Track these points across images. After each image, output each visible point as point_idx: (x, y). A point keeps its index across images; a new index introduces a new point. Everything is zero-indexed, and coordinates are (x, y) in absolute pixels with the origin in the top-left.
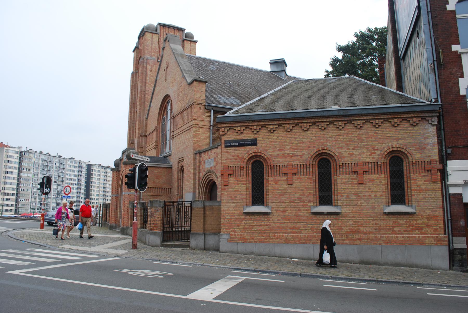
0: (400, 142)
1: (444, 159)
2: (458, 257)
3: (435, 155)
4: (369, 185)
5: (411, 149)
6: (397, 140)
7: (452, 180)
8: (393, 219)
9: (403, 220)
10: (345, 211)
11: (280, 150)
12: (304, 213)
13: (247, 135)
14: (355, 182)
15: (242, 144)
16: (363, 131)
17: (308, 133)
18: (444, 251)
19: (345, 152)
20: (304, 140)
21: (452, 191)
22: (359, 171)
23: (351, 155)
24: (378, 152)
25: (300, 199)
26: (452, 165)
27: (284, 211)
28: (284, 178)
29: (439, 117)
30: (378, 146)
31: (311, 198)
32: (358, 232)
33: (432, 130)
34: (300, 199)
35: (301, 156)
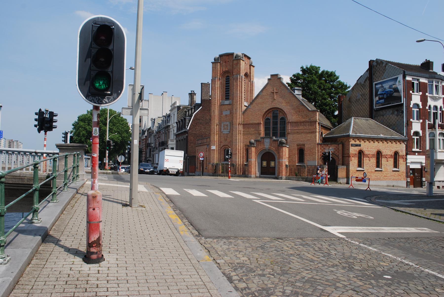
1: (407, 154)
2: (408, 184)
3: (405, 154)
5: (400, 151)
7: (408, 161)
8: (395, 172)
9: (397, 173)
12: (373, 171)
13: (358, 142)
15: (357, 145)
16: (388, 144)
18: (405, 182)
21: (408, 164)
26: (408, 156)
28: (368, 158)
29: (407, 142)
30: (392, 149)
31: (375, 165)
32: (386, 177)
33: (405, 146)
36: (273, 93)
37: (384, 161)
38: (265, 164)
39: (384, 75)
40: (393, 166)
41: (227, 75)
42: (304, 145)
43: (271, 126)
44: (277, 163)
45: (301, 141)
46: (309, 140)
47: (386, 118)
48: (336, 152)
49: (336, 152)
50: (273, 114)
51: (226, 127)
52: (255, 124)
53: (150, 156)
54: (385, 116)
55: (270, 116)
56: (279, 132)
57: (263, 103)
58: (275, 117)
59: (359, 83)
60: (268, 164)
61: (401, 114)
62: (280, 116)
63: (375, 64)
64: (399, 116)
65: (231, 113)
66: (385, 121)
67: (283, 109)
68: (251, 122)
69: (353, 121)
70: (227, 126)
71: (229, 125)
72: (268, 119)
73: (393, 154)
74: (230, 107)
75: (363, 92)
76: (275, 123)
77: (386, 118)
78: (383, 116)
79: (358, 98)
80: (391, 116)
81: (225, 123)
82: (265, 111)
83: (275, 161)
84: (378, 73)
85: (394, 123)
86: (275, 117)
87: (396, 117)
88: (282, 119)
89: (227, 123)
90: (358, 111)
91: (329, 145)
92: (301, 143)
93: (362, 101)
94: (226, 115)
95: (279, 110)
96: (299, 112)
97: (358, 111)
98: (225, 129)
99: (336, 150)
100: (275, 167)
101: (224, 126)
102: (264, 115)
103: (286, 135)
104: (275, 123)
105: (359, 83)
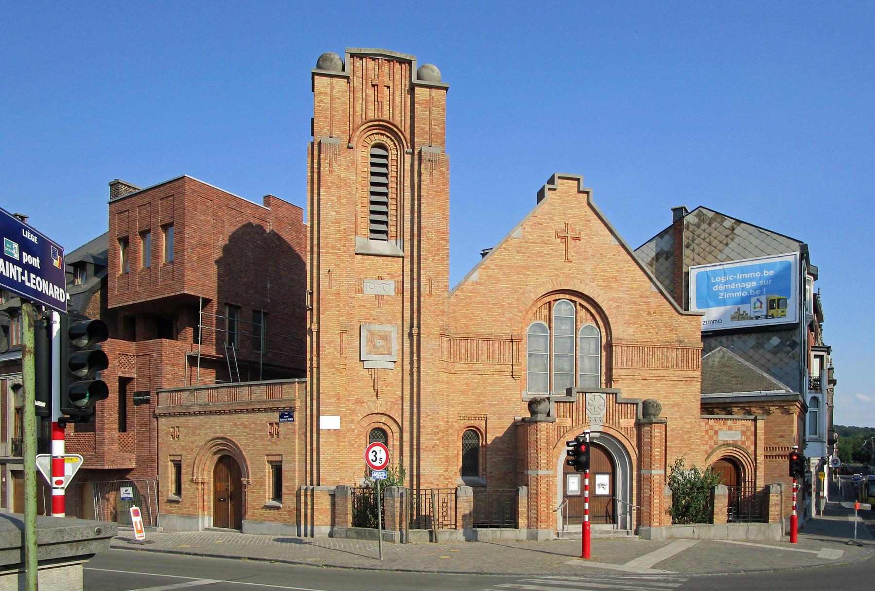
39: (727, 251)
51: (379, 343)
57: (528, 268)
61: (789, 349)
63: (690, 219)
67: (598, 300)
68: (483, 330)
70: (386, 338)
81: (376, 327)
84: (704, 245)
87: (769, 356)
89: (388, 328)
91: (729, 422)
94: (379, 297)
98: (375, 349)
99: (748, 438)
101: (370, 341)
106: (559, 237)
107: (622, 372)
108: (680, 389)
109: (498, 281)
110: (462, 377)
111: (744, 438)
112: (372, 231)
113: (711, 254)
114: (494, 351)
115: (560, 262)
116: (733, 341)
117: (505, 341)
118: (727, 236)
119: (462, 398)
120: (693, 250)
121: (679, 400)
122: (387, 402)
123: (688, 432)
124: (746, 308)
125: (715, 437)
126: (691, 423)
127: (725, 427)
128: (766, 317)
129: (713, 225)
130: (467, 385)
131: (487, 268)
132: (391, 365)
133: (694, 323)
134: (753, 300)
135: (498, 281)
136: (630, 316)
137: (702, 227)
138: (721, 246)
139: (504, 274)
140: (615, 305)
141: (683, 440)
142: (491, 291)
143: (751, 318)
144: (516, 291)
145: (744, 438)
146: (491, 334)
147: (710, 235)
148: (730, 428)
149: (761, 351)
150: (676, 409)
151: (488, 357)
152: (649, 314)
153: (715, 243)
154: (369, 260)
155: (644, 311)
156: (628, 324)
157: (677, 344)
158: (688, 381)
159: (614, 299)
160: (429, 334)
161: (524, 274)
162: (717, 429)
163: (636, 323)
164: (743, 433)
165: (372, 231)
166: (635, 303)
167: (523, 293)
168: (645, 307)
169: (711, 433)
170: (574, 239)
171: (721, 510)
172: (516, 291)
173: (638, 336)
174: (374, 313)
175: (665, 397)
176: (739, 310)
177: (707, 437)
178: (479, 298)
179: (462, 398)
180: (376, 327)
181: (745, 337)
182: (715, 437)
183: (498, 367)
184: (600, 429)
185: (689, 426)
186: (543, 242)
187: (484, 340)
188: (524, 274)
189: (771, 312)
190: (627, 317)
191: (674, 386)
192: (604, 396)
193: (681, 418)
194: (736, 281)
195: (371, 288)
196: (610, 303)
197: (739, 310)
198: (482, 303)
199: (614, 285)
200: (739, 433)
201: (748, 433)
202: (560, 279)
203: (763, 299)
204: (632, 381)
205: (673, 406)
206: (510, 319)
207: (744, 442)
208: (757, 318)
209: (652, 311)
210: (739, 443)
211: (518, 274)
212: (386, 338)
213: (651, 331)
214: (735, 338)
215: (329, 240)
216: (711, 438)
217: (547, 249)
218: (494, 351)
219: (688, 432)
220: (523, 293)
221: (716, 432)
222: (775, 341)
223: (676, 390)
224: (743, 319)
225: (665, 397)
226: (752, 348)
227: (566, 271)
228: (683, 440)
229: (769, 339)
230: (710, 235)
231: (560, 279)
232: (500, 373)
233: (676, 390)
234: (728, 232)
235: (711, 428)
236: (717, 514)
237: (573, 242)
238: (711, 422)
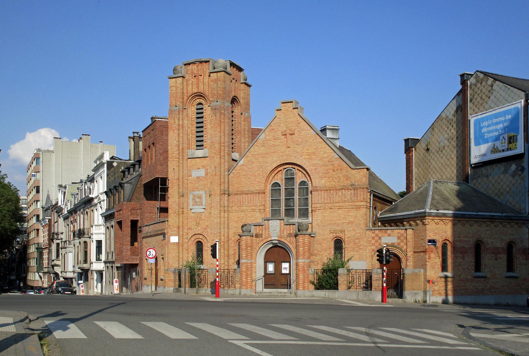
0: (514, 236)
4: (500, 260)
6: (512, 235)
10: (489, 275)
11: (459, 237)
14: (494, 259)
17: (473, 227)
19: (490, 241)
20: (470, 232)
22: (496, 252)
23: (492, 242)
24: (504, 242)
25: (468, 268)
27: (460, 276)
31: (473, 268)
34: (468, 268)
35: (469, 242)
36: (286, 135)
37: (486, 259)
38: (271, 268)
40: (505, 269)
41: (198, 101)
42: (343, 231)
43: (283, 197)
44: (293, 267)
45: (338, 225)
46: (351, 222)
47: (493, 181)
48: (402, 244)
49: (402, 244)
50: (286, 175)
52: (252, 193)
53: (58, 256)
54: (490, 178)
55: (280, 178)
56: (296, 208)
57: (267, 154)
58: (290, 180)
59: (444, 115)
60: (278, 268)
62: (299, 177)
64: (517, 177)
65: (207, 174)
66: (491, 186)
68: (245, 189)
69: (431, 188)
70: (200, 197)
71: (204, 196)
72: (276, 184)
73: (505, 247)
74: (205, 162)
75: (451, 134)
76: (290, 193)
77: (493, 181)
78: (487, 176)
79: (442, 144)
80: (502, 176)
81: (196, 193)
82: (271, 169)
83: (290, 262)
85: (508, 189)
86: (290, 180)
87: (511, 179)
88: (303, 183)
89: (201, 192)
90: (442, 168)
91: (389, 232)
92: (338, 228)
93: (448, 150)
94: (198, 178)
95: (296, 167)
96: (334, 171)
97: (442, 168)
98: (195, 203)
99: (402, 241)
100: (290, 274)
101: (194, 199)
102: (268, 177)
103: (310, 215)
104: (290, 193)
105: (444, 115)
106: (283, 135)
107: (318, 205)
108: (353, 213)
109: (253, 163)
110: (236, 214)
111: (399, 241)
112: (197, 146)
113: (482, 107)
114: (251, 200)
115: (284, 149)
116: (493, 169)
117: (256, 193)
118: (489, 91)
119: (236, 225)
120: (473, 103)
121: (352, 219)
122: (201, 228)
123: (358, 239)
124: (498, 144)
125: (379, 241)
126: (360, 233)
127: (386, 235)
128: (508, 149)
129: (483, 84)
130: (238, 218)
131: (248, 156)
132: (203, 211)
133: (362, 173)
134: (501, 137)
135: (253, 163)
136: (323, 173)
137: (478, 86)
138: (487, 99)
139: (256, 159)
140: (314, 168)
141: (355, 243)
142: (249, 169)
143: (500, 151)
144: (262, 167)
145: (399, 241)
146: (248, 191)
147: (481, 91)
148: (389, 235)
149: (507, 175)
150: (350, 225)
151: (248, 203)
152: (334, 171)
153: (484, 97)
154: (193, 161)
155: (330, 169)
156: (321, 178)
157: (350, 187)
158: (358, 208)
159: (314, 165)
160: (215, 194)
161: (266, 157)
162: (380, 235)
163: (326, 177)
164: (399, 238)
165: (197, 146)
166: (325, 166)
167: (265, 168)
168: (331, 167)
169: (376, 238)
170: (291, 134)
171: (342, 282)
172: (262, 167)
173: (328, 184)
174: (196, 186)
175: (344, 218)
176: (494, 145)
177: (373, 241)
178: (244, 173)
179: (236, 225)
180: (196, 193)
181: (499, 165)
182: (379, 241)
183: (253, 207)
184: (277, 238)
185: (359, 235)
186: (275, 139)
187: (246, 194)
188: (266, 157)
189: (511, 145)
190: (321, 174)
191: (349, 211)
192: (278, 221)
193: (354, 230)
194: (493, 124)
195: (195, 174)
196: (311, 167)
197: (494, 145)
198: (245, 175)
199: (314, 157)
200: (396, 238)
201: (402, 238)
202: (284, 158)
203: (506, 136)
204: (325, 211)
205: (349, 223)
206: (259, 182)
207: (399, 244)
208: (503, 151)
209: (335, 169)
210: (396, 244)
211: (263, 157)
212: (200, 197)
213: (335, 180)
214: (494, 166)
215: (174, 155)
216: (376, 241)
217: (277, 142)
218: (251, 200)
219: (358, 239)
220: (265, 168)
221: (380, 238)
222: (514, 167)
223: (351, 214)
224: (497, 152)
225: (344, 218)
226: (503, 173)
227: (287, 153)
228: (355, 243)
229: (510, 166)
230: (481, 91)
231: (284, 158)
232: (254, 210)
233: (351, 214)
234: (490, 88)
235: (377, 235)
236: (340, 284)
237: (290, 136)
238: (377, 232)
